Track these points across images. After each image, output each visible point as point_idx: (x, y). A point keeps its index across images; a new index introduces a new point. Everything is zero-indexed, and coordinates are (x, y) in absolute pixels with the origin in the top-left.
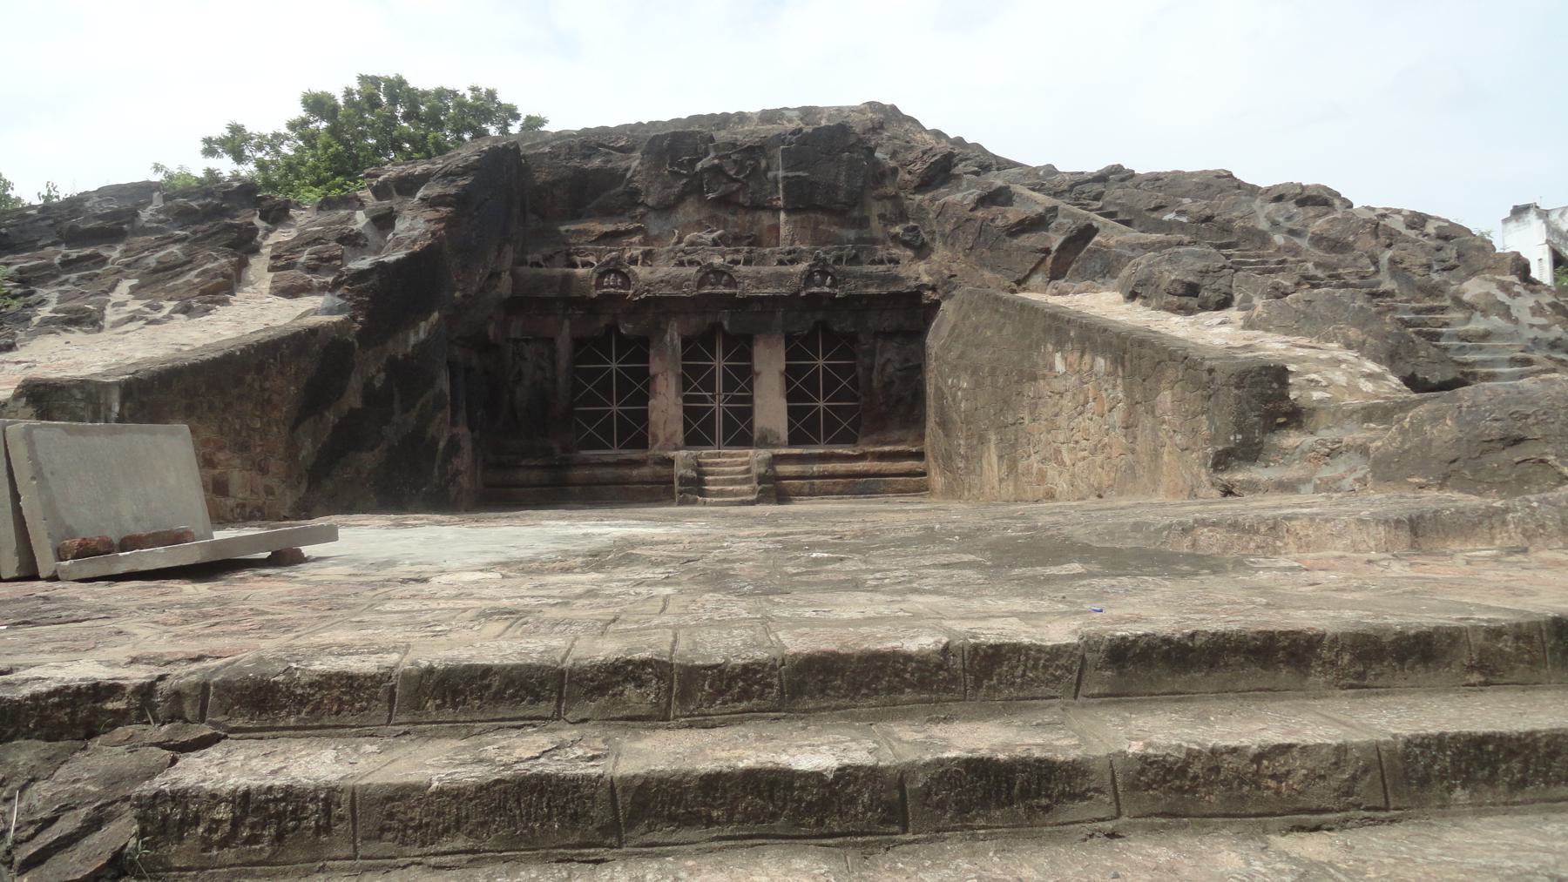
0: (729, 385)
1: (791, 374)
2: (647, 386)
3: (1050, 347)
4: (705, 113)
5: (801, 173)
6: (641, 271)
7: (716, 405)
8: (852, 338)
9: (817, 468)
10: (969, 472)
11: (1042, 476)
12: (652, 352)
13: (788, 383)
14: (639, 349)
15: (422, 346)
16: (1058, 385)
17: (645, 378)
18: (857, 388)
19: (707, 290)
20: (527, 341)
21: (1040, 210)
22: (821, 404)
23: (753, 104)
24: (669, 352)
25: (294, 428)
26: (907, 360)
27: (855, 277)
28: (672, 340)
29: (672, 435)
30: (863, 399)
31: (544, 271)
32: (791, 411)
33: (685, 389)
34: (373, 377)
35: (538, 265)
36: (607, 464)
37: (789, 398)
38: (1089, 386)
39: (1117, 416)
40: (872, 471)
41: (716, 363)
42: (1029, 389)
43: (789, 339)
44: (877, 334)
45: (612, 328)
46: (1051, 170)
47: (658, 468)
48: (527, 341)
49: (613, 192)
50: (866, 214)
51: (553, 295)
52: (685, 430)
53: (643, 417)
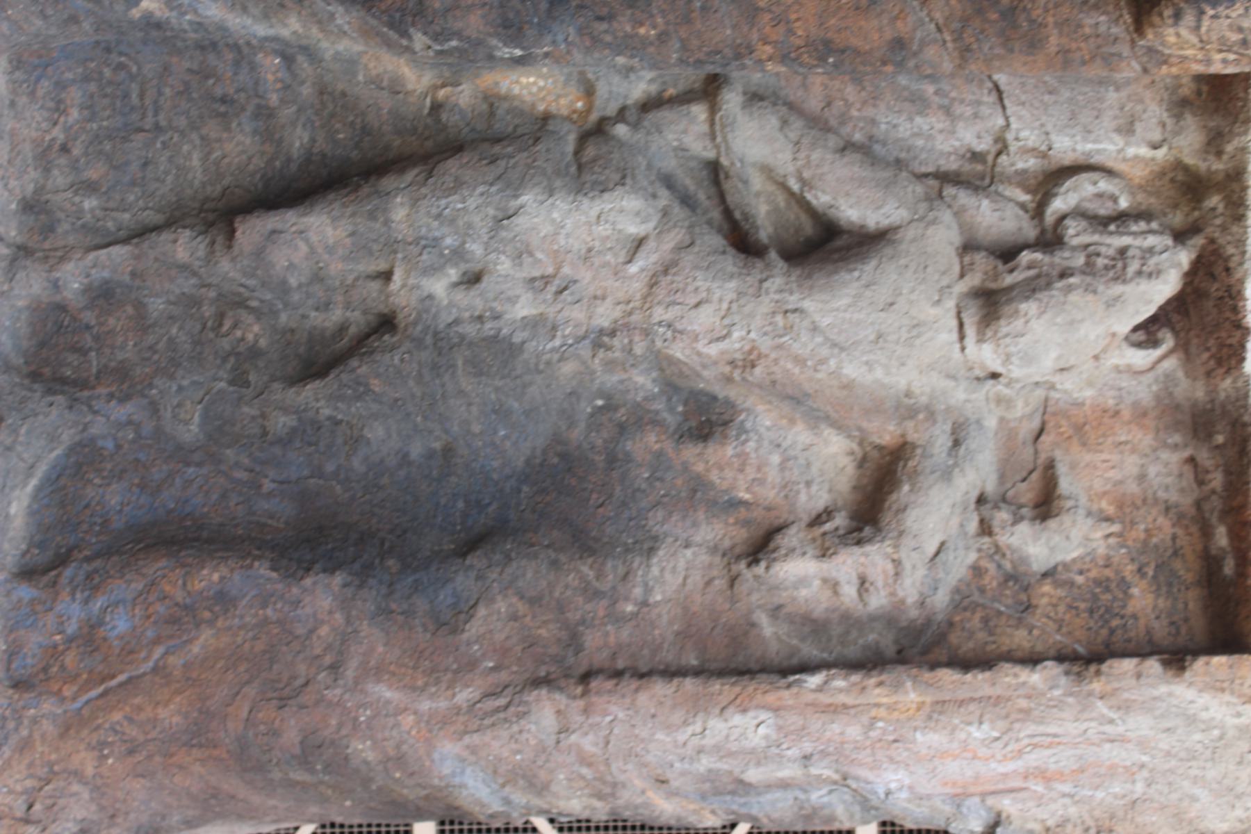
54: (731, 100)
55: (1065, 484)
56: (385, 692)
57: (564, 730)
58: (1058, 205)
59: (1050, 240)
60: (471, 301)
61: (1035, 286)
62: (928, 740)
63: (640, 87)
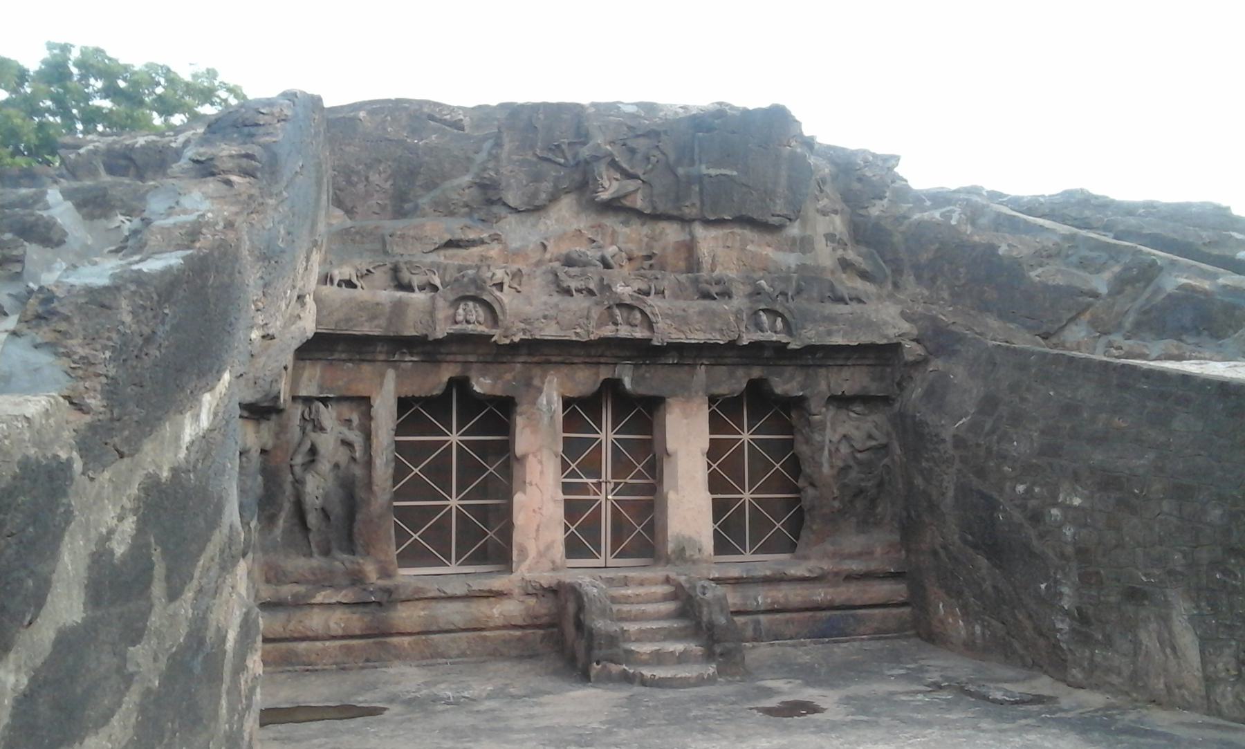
0: (621, 466)
1: (714, 451)
5: (728, 172)
7: (602, 497)
9: (763, 597)
12: (520, 421)
17: (504, 452)
19: (608, 331)
20: (324, 401)
21: (1056, 239)
22: (747, 496)
24: (546, 420)
26: (870, 437)
27: (815, 321)
28: (549, 403)
29: (549, 547)
31: (362, 293)
32: (719, 509)
35: (350, 284)
40: (838, 602)
41: (602, 436)
44: (841, 401)
45: (460, 384)
47: (532, 601)
48: (324, 401)
49: (456, 182)
50: (809, 233)
51: (377, 332)
53: (503, 518)
54: (293, 463)
55: (347, 418)
56: (372, 509)
57: (377, 485)
58: (307, 418)
59: (313, 420)
60: (320, 498)
61: (320, 423)
62: (381, 439)
63: (291, 476)
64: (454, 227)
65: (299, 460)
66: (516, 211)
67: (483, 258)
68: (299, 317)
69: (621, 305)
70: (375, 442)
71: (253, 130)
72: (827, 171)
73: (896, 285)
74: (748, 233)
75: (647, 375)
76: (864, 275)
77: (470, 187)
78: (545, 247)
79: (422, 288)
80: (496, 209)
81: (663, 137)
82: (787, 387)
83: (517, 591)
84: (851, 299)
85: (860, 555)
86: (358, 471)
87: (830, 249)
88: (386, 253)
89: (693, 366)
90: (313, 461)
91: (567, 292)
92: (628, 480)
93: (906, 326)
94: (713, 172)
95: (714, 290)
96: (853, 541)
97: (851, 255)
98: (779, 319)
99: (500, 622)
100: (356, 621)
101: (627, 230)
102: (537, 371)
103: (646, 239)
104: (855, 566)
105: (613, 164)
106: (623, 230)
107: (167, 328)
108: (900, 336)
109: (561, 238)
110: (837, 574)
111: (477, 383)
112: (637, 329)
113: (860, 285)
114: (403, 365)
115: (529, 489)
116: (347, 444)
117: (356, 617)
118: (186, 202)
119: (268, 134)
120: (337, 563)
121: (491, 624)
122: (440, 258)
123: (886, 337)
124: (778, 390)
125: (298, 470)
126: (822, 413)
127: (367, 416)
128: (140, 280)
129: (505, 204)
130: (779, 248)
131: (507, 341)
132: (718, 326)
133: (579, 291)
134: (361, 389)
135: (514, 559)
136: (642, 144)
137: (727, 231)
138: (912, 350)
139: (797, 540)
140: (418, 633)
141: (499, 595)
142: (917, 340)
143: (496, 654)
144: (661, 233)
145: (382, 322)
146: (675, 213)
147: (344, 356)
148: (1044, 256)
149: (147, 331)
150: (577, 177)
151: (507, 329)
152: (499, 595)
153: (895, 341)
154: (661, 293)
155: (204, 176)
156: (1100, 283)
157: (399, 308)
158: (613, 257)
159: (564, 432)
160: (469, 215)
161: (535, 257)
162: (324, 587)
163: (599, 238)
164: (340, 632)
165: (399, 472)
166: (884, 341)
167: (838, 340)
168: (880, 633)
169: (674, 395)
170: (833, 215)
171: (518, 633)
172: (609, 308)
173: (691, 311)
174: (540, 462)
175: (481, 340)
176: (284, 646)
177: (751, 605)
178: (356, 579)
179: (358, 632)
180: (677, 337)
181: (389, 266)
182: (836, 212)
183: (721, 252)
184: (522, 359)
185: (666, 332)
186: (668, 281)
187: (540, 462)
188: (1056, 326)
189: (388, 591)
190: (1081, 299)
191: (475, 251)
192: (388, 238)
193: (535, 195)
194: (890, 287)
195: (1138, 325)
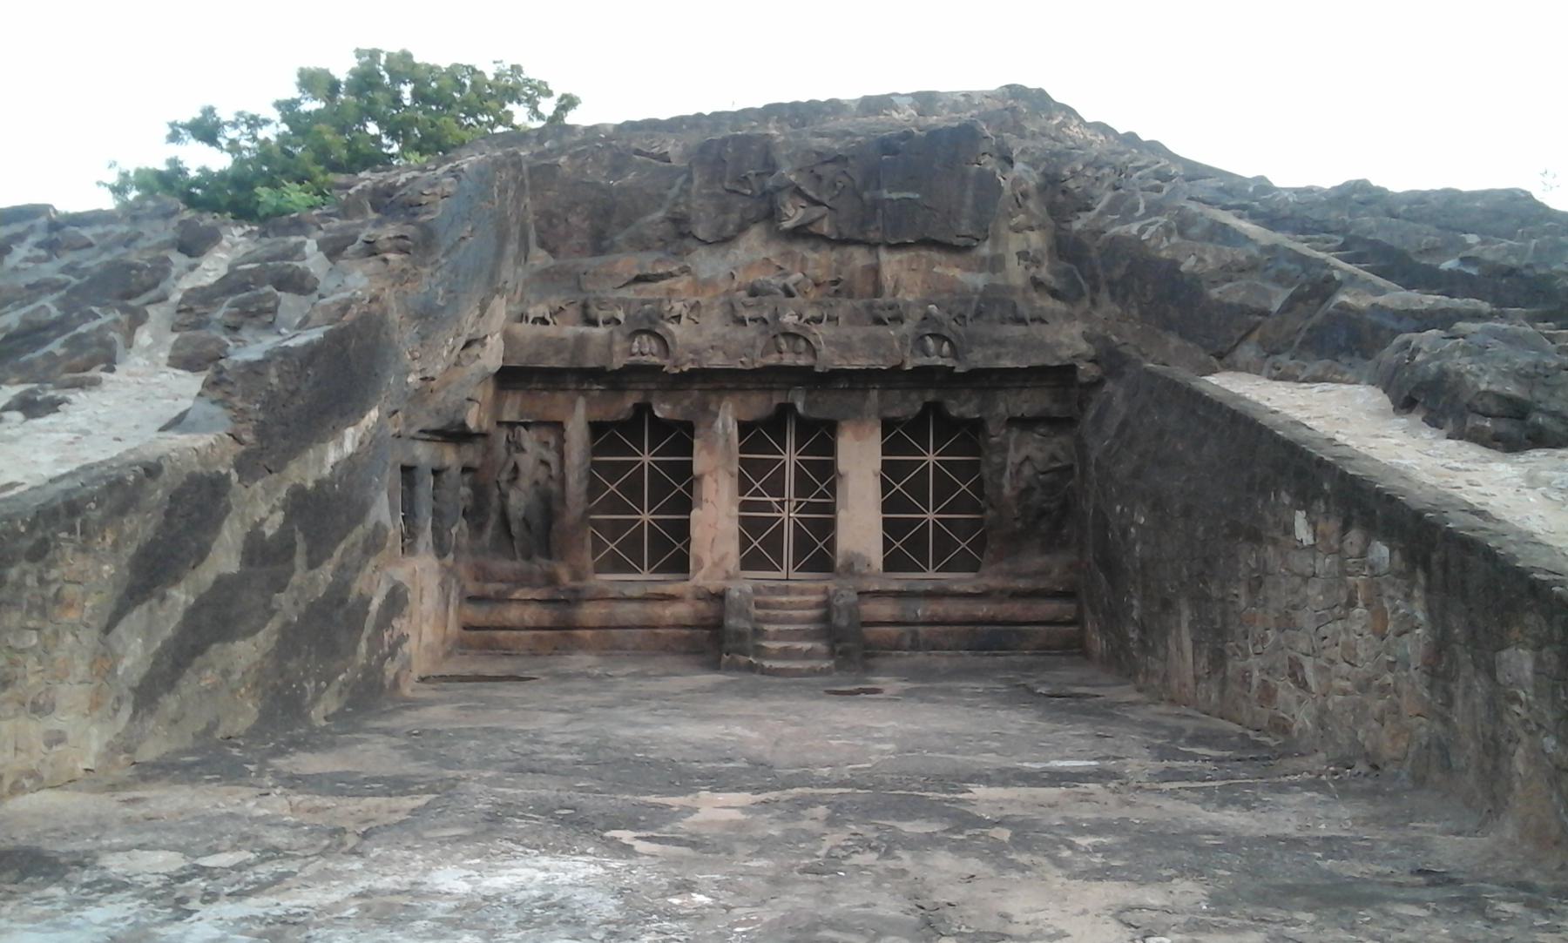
0: (803, 487)
1: (890, 471)
2: (689, 488)
3: (1286, 499)
4: (787, 99)
5: (911, 195)
6: (679, 332)
7: (784, 515)
8: (977, 426)
9: (923, 610)
10: (1145, 648)
11: (1268, 695)
12: (697, 443)
13: (886, 487)
14: (679, 437)
15: (350, 464)
16: (1301, 562)
18: (981, 496)
19: (772, 360)
20: (526, 425)
22: (931, 516)
23: (850, 90)
24: (721, 442)
25: (108, 629)
26: (1054, 458)
27: (982, 345)
28: (725, 426)
29: (723, 558)
30: (989, 512)
31: (550, 331)
32: (887, 525)
33: (742, 494)
34: (263, 521)
35: (544, 321)
36: (630, 599)
37: (886, 507)
38: (1359, 580)
39: (1415, 645)
40: (1000, 617)
41: (786, 457)
42: (1248, 558)
43: (887, 426)
44: (1015, 422)
45: (643, 409)
46: (1263, 185)
47: (701, 605)
49: (650, 218)
50: (1000, 251)
52: (742, 549)
64: (647, 262)
65: (504, 477)
66: (704, 242)
67: (670, 292)
68: (478, 356)
69: (786, 334)
70: (567, 462)
71: (417, 209)
72: (1032, 183)
73: (1093, 302)
74: (935, 255)
75: (820, 400)
76: (1055, 294)
77: (663, 222)
78: (733, 276)
79: (606, 323)
80: (687, 242)
81: (851, 162)
82: (963, 409)
83: (689, 596)
84: (1033, 320)
85: (1036, 574)
86: (554, 487)
87: (1022, 267)
88: (581, 290)
89: (866, 390)
90: (515, 479)
91: (741, 322)
92: (810, 499)
93: (1083, 347)
94: (894, 196)
95: (885, 315)
96: (1035, 561)
97: (1044, 273)
98: (946, 345)
99: (671, 621)
100: (546, 615)
101: (816, 256)
102: (713, 397)
103: (834, 264)
104: (1022, 584)
105: (798, 191)
106: (812, 256)
107: (310, 384)
108: (1074, 357)
109: (750, 266)
110: (1002, 591)
111: (659, 409)
112: (802, 357)
113: (1049, 303)
114: (592, 393)
115: (705, 505)
116: (545, 463)
117: (546, 611)
118: (350, 281)
119: (427, 213)
120: (536, 567)
121: (663, 623)
122: (629, 294)
123: (1058, 358)
124: (954, 413)
125: (503, 485)
126: (996, 433)
127: (562, 440)
128: (286, 353)
129: (695, 237)
130: (968, 269)
131: (677, 371)
132: (881, 351)
133: (753, 320)
134: (555, 415)
135: (691, 567)
136: (828, 170)
137: (913, 254)
138: (1086, 371)
139: (981, 556)
140: (600, 628)
141: (672, 598)
142: (1094, 361)
143: (667, 648)
144: (850, 258)
145: (567, 355)
146: (860, 238)
147: (540, 386)
148: (1230, 271)
149: (291, 387)
150: (764, 206)
151: (677, 360)
152: (672, 598)
153: (1069, 362)
154: (833, 319)
155: (370, 255)
156: (1278, 298)
157: (581, 341)
158: (795, 285)
159: (741, 452)
160: (664, 248)
161: (723, 287)
162: (523, 586)
163: (788, 267)
164: (532, 624)
165: (594, 489)
166: (1056, 363)
167: (1007, 363)
168: (1045, 648)
169: (845, 418)
170: (1028, 232)
171: (686, 632)
172: (775, 337)
173: (855, 338)
174: (716, 481)
175: (656, 370)
176: (486, 633)
177: (910, 617)
178: (551, 580)
179: (547, 624)
180: (839, 363)
181: (579, 303)
182: (1031, 229)
183: (904, 275)
184: (697, 386)
185: (829, 358)
186: (844, 307)
187: (716, 481)
188: (1228, 346)
189: (575, 591)
190: (1251, 317)
191: (663, 284)
192: (582, 277)
193: (723, 226)
194: (1087, 303)
195: (1304, 343)
